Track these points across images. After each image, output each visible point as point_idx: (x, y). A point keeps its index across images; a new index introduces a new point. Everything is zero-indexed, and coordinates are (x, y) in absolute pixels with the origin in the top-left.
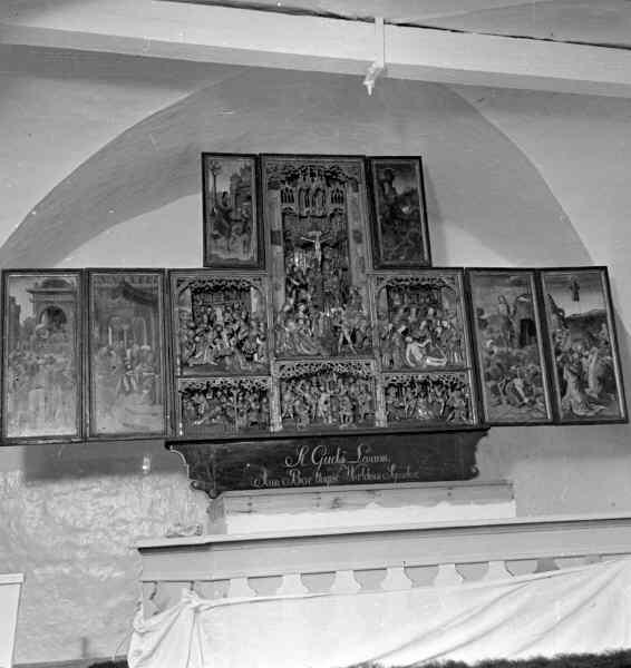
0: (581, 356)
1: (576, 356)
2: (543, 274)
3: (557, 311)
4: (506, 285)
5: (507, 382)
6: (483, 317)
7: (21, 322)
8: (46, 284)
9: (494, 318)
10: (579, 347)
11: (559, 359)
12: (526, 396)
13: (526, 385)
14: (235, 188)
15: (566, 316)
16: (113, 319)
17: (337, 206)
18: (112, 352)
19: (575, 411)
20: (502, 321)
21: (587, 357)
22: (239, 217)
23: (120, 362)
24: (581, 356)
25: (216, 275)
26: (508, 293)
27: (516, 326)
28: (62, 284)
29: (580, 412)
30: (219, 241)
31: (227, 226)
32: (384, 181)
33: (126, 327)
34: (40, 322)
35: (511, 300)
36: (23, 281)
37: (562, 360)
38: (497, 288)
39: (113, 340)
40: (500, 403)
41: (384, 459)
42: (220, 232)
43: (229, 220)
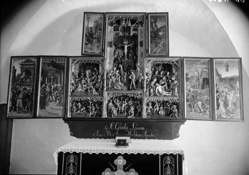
0: (227, 94)
1: (225, 94)
2: (214, 60)
3: (218, 75)
4: (201, 64)
5: (195, 102)
6: (188, 77)
7: (16, 75)
8: (25, 62)
9: (192, 77)
10: (226, 90)
11: (217, 94)
12: (203, 109)
13: (203, 104)
14: (95, 25)
15: (222, 78)
16: (48, 74)
17: (135, 32)
18: (47, 87)
19: (222, 116)
20: (195, 78)
21: (229, 94)
22: (96, 37)
23: (49, 90)
24: (227, 94)
25: (86, 59)
26: (199, 67)
27: (201, 80)
28: (31, 61)
29: (224, 116)
30: (88, 46)
31: (91, 39)
32: (153, 22)
33: (52, 77)
34: (22, 75)
35: (200, 70)
36: (18, 60)
37: (218, 95)
38: (195, 65)
39: (47, 82)
40: (191, 111)
41: (143, 129)
42: (88, 42)
43: (92, 38)
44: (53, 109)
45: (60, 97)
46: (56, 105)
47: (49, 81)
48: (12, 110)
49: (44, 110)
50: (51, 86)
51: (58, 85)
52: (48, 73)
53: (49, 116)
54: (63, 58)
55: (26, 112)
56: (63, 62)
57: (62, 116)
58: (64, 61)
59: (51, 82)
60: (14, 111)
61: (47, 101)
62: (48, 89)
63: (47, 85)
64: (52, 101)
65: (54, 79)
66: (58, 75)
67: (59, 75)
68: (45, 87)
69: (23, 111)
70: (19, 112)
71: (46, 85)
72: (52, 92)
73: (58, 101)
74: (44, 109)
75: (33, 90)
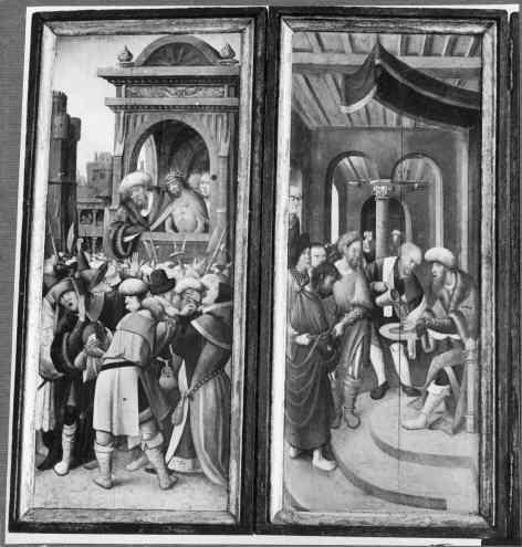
18: (341, 265)
23: (360, 295)
33: (381, 189)
39: (342, 231)
44: (398, 454)
45: (448, 354)
46: (420, 421)
47: (355, 218)
48: (59, 458)
49: (326, 465)
50: (370, 257)
51: (431, 254)
52: (348, 154)
53: (355, 517)
54: (462, 30)
55: (174, 480)
56: (471, 63)
57: (477, 520)
58: (477, 51)
59: (373, 228)
60: (72, 466)
61: (348, 391)
62: (349, 288)
63: (339, 256)
64: (386, 387)
65: (393, 204)
66: (426, 168)
67: (435, 171)
68: (327, 268)
69: (153, 471)
70: (118, 475)
71: (334, 254)
72: (388, 312)
73: (435, 391)
74: (328, 454)
75: (226, 293)
